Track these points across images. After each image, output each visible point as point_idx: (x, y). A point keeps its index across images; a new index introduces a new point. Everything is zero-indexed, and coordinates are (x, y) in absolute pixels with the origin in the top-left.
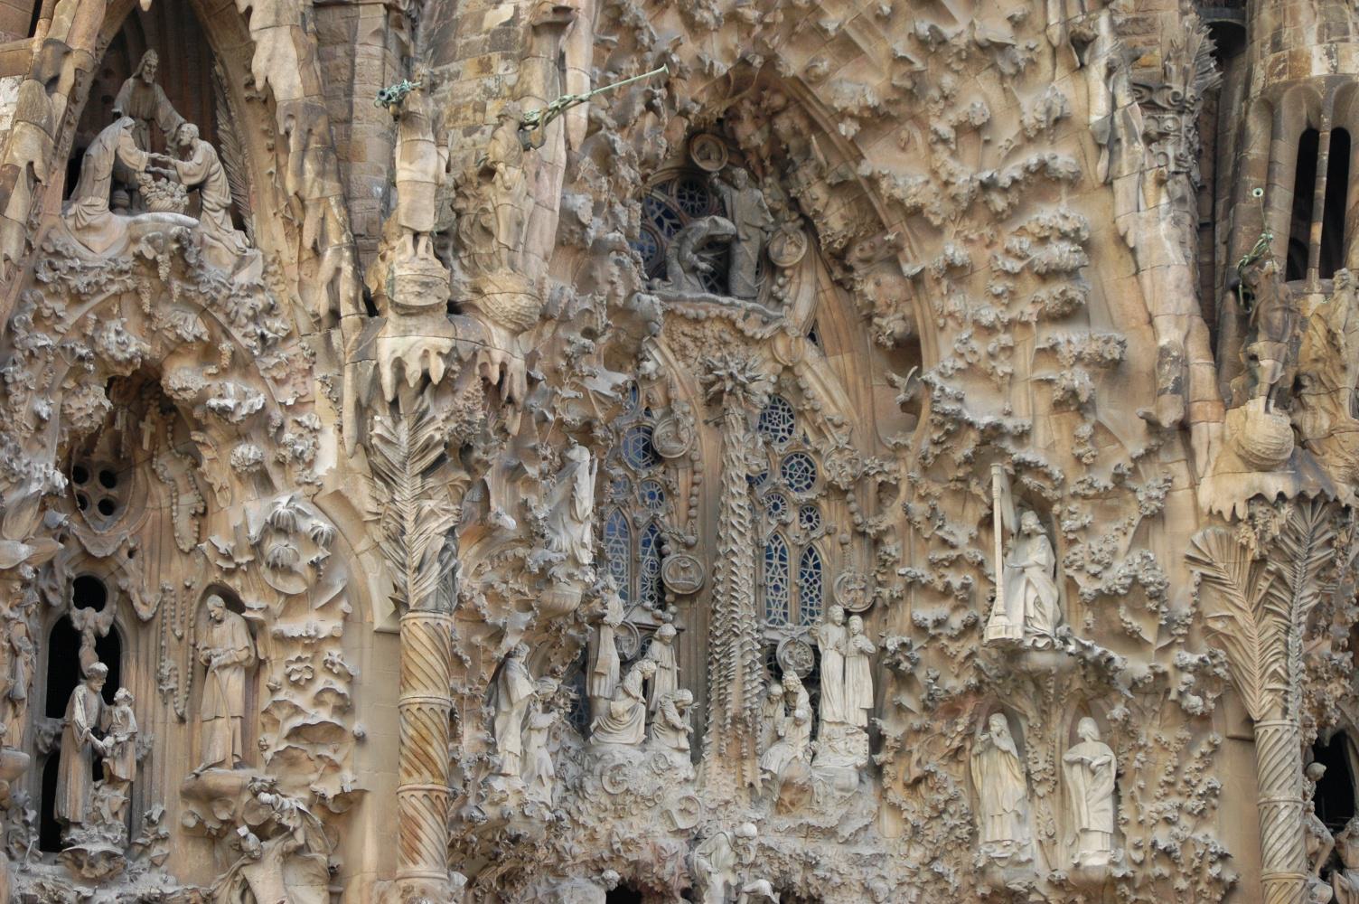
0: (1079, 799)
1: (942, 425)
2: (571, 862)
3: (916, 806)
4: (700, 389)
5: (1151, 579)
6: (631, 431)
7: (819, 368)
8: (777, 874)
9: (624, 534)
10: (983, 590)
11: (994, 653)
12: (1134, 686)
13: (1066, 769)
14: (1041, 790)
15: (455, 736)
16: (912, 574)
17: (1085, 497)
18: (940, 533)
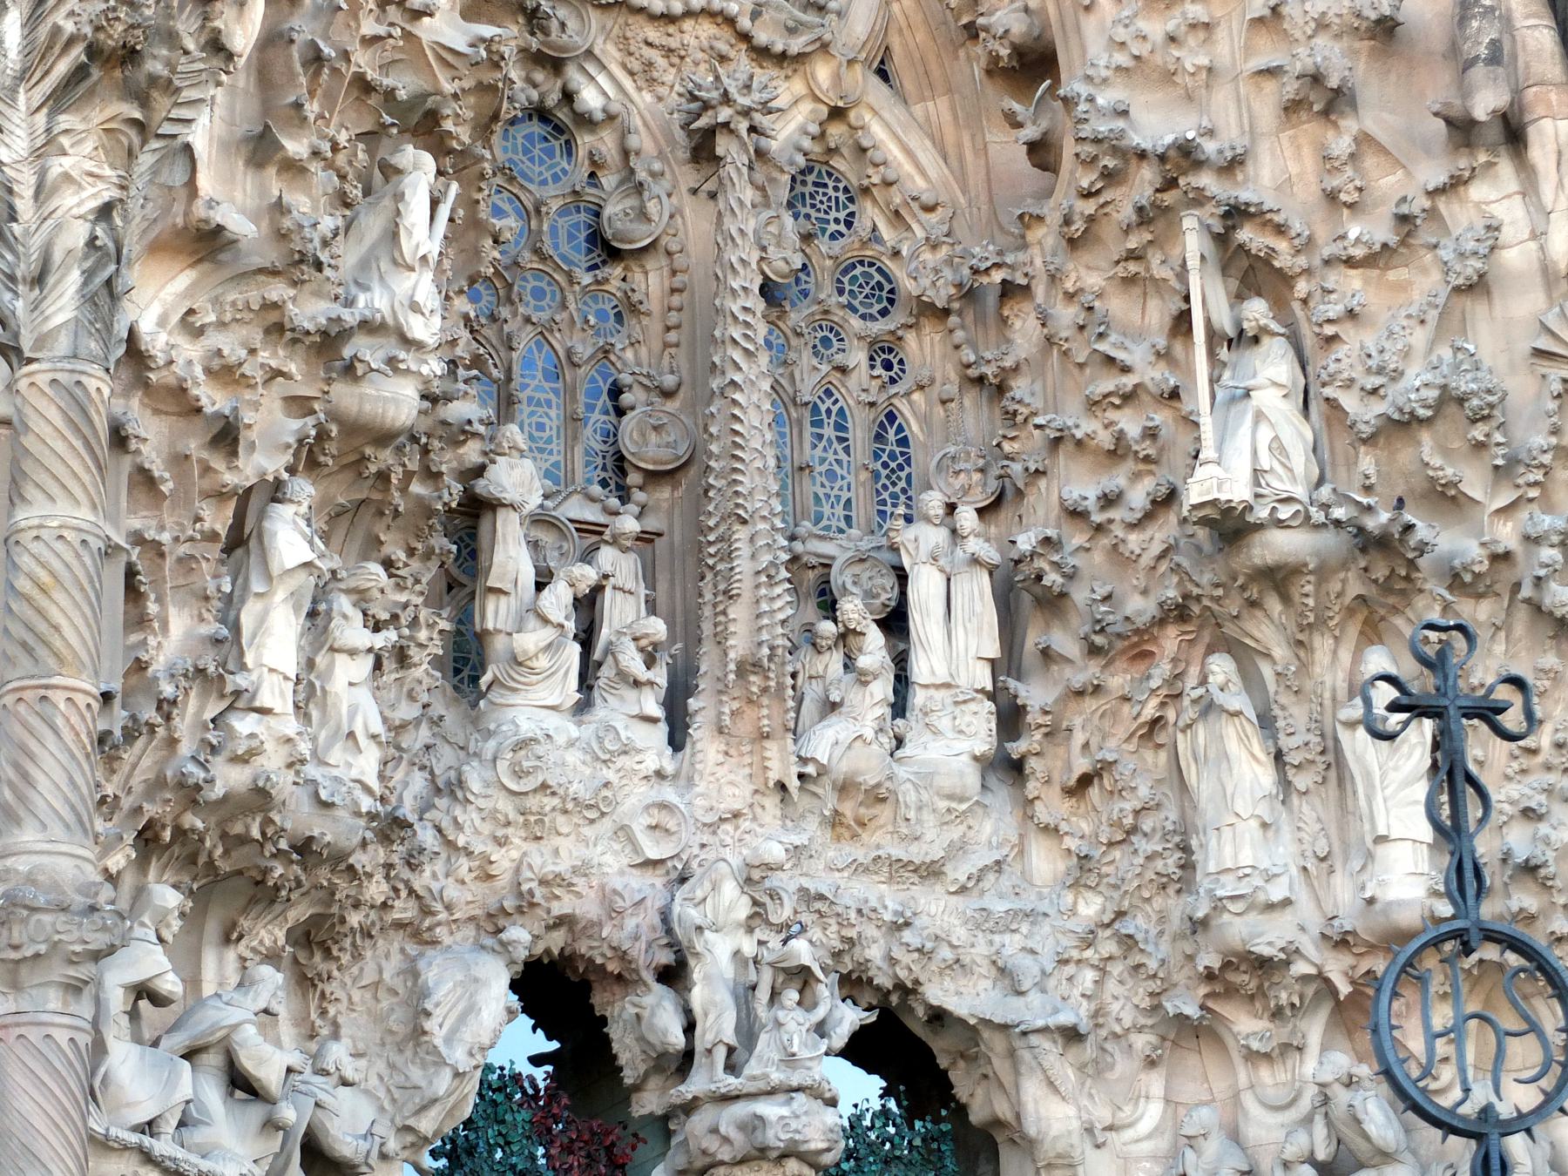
0: (1370, 786)
1: (1095, 159)
2: (443, 916)
3: (1085, 827)
4: (680, 135)
5: (1474, 386)
6: (563, 211)
7: (893, 112)
8: (839, 946)
9: (548, 376)
10: (1185, 441)
11: (1202, 533)
12: (1458, 580)
13: (1344, 735)
14: (1301, 781)
15: (138, 620)
16: (1057, 424)
17: (1350, 262)
18: (1103, 347)
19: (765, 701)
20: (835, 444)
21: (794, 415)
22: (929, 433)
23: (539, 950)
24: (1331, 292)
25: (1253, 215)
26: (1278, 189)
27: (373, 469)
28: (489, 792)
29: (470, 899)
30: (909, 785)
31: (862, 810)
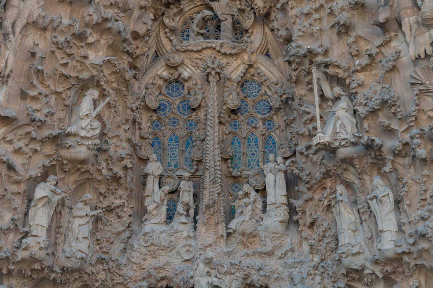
1: (294, 60)
2: (129, 280)
5: (388, 97)
6: (181, 102)
9: (177, 141)
17: (357, 71)
18: (302, 108)
19: (216, 214)
20: (254, 146)
21: (242, 141)
22: (280, 139)
23: (159, 285)
24: (354, 80)
25: (329, 65)
26: (340, 56)
27: (83, 170)
28: (140, 247)
29: (138, 275)
30: (262, 231)
31: (250, 240)
